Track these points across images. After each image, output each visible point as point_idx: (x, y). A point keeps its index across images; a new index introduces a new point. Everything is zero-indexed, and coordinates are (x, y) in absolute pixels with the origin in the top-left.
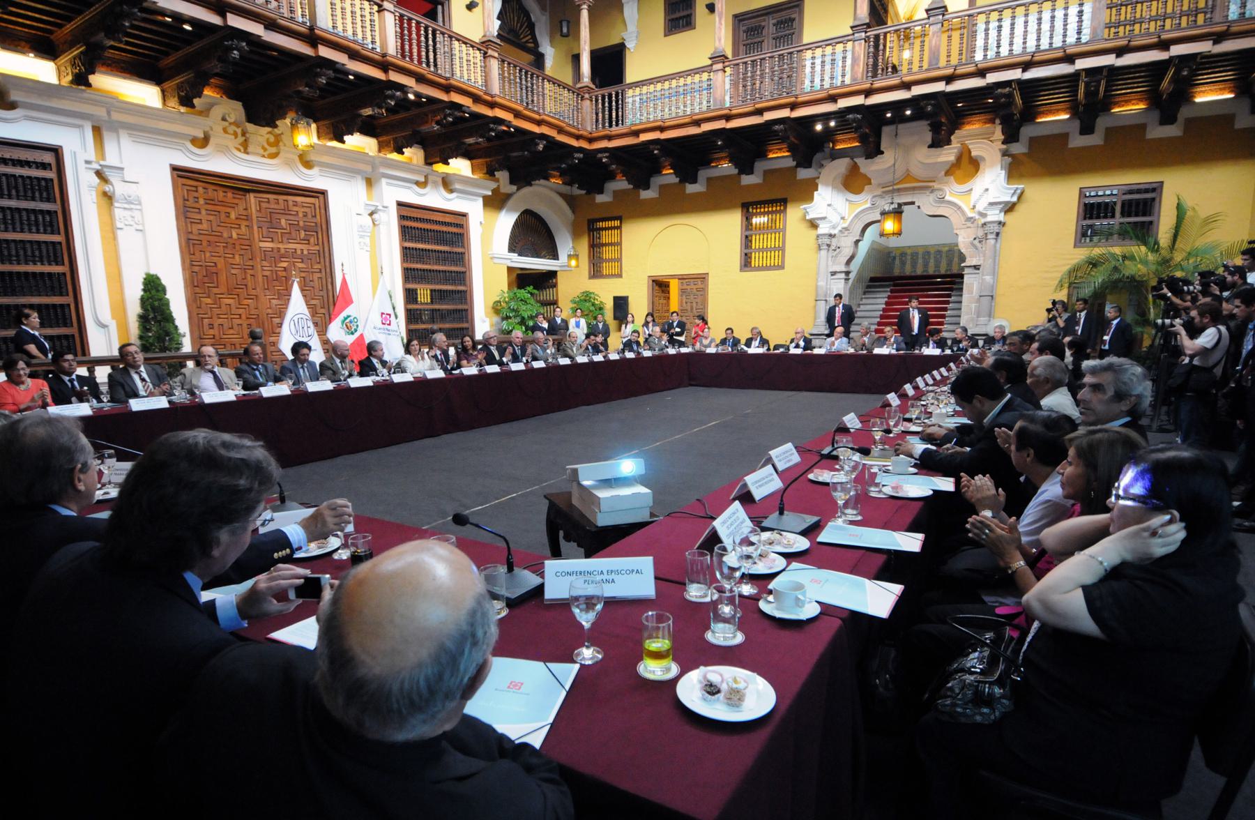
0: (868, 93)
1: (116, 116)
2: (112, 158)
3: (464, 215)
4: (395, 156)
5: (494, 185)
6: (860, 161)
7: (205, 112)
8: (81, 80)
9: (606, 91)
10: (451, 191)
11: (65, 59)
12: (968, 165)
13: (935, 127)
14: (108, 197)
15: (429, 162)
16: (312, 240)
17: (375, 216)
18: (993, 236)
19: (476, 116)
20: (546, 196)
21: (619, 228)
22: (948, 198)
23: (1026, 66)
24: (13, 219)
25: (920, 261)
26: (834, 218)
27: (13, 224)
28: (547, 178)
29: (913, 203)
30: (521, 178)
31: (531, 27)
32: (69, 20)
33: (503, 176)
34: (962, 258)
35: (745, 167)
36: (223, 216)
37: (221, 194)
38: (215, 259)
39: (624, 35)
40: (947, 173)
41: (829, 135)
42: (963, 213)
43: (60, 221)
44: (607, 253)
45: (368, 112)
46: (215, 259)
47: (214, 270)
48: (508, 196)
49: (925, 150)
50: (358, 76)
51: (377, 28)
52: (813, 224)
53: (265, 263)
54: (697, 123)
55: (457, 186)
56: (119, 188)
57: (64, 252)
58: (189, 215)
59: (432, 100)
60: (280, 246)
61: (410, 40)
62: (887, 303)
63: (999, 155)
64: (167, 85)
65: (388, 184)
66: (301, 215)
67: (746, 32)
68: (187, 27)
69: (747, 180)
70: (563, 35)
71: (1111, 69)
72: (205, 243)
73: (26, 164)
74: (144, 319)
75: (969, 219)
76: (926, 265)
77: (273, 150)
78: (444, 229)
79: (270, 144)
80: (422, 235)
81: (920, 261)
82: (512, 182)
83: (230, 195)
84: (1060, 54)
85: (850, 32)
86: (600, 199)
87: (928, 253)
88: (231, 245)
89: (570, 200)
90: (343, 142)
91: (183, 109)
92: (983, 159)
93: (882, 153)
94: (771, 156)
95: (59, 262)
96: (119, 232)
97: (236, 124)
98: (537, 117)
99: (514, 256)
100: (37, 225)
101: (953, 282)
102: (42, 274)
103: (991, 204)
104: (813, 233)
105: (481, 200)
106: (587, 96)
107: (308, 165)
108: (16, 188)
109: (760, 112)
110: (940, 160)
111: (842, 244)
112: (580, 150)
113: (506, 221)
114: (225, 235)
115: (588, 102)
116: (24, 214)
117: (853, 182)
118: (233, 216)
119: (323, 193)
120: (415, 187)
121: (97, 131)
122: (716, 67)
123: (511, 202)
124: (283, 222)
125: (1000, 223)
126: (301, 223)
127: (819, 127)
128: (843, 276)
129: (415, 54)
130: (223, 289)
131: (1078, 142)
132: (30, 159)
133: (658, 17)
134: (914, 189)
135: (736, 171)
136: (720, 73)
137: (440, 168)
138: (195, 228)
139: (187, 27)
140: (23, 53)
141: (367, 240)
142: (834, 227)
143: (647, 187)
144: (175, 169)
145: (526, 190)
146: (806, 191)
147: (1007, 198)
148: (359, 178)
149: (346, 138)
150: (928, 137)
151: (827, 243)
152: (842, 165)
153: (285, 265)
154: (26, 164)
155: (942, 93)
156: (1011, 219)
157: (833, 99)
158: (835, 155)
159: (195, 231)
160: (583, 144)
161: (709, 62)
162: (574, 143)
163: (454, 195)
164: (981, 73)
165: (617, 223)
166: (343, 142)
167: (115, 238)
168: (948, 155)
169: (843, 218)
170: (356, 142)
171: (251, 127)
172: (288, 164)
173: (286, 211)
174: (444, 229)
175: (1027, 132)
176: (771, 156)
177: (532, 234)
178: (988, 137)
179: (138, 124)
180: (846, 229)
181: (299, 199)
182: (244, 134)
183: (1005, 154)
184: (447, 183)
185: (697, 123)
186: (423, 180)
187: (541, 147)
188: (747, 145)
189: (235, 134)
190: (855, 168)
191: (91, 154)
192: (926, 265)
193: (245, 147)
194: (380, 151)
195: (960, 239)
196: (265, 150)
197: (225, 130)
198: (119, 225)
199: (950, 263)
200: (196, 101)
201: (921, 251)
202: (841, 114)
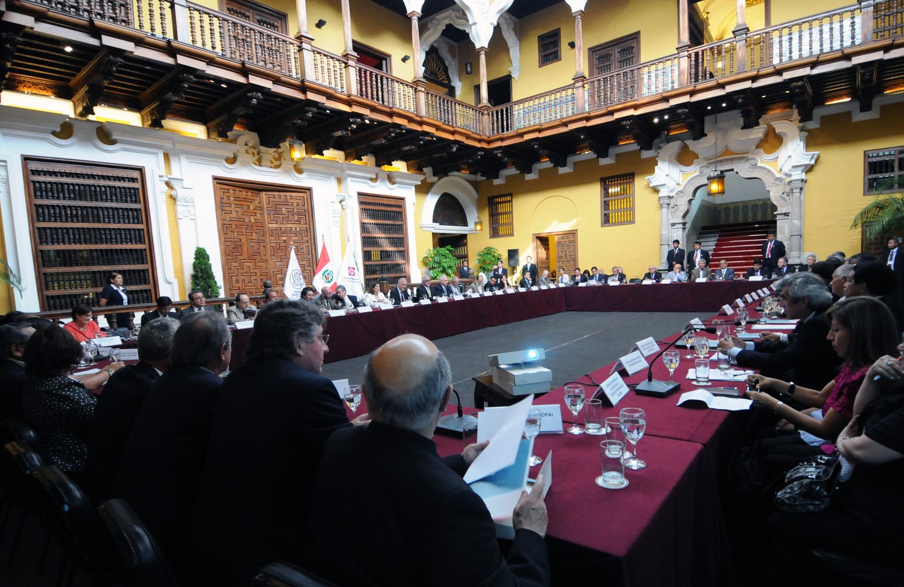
0: (692, 93)
3: (403, 199)
4: (356, 162)
5: (422, 177)
6: (690, 143)
7: (234, 141)
8: (156, 124)
9: (499, 108)
10: (393, 183)
11: (146, 111)
12: (773, 141)
13: (746, 115)
14: (173, 198)
15: (379, 164)
17: (343, 203)
18: (798, 190)
19: (410, 131)
20: (457, 183)
21: (511, 201)
22: (759, 164)
23: (813, 65)
24: (113, 215)
25: (741, 213)
26: (672, 185)
27: (114, 218)
28: (459, 171)
29: (732, 170)
30: (441, 171)
31: (446, 69)
32: (149, 85)
33: (428, 170)
34: (774, 208)
35: (602, 153)
36: (245, 208)
37: (244, 193)
38: (240, 237)
39: (510, 69)
40: (758, 147)
41: (664, 125)
42: (773, 174)
43: (142, 215)
44: (502, 219)
45: (339, 133)
46: (240, 237)
47: (239, 243)
48: (432, 184)
49: (739, 131)
50: (333, 111)
51: (344, 78)
52: (656, 190)
53: (272, 238)
54: (565, 124)
55: (398, 180)
56: (180, 193)
57: (145, 236)
58: (224, 208)
59: (381, 123)
61: (366, 85)
62: (716, 245)
63: (797, 131)
64: (211, 124)
67: (598, 59)
68: (224, 86)
69: (603, 162)
70: (468, 73)
71: (881, 62)
72: (234, 226)
74: (195, 277)
75: (778, 179)
76: (746, 215)
77: (277, 163)
78: (389, 209)
79: (275, 159)
81: (741, 213)
82: (435, 174)
83: (249, 194)
84: (839, 54)
85: (676, 52)
86: (496, 182)
87: (747, 206)
88: (249, 226)
90: (323, 155)
91: (220, 139)
92: (785, 134)
93: (706, 135)
94: (621, 143)
95: (141, 241)
97: (253, 147)
98: (451, 129)
99: (437, 225)
100: (129, 218)
101: (770, 226)
102: (131, 250)
103: (794, 167)
104: (656, 196)
105: (414, 188)
106: (486, 112)
107: (300, 171)
108: (116, 195)
109: (611, 113)
110: (752, 137)
111: (679, 203)
112: (482, 149)
113: (431, 201)
114: (247, 220)
115: (487, 117)
116: (121, 211)
117: (684, 158)
118: (251, 208)
119: (309, 189)
120: (370, 182)
122: (577, 85)
123: (434, 188)
124: (284, 210)
125: (802, 180)
127: (656, 120)
128: (681, 226)
129: (369, 93)
130: (245, 256)
131: (859, 117)
132: (125, 176)
133: (534, 54)
134: (732, 159)
135: (595, 156)
136: (581, 89)
137: (386, 168)
138: (228, 217)
139: (224, 86)
140: (121, 108)
141: (338, 219)
142: (672, 191)
143: (530, 172)
144: (219, 181)
145: (445, 179)
146: (649, 167)
147: (807, 162)
148: (333, 178)
149: (324, 152)
150: (741, 122)
151: (668, 203)
152: (675, 146)
153: (285, 238)
155: (750, 89)
156: (810, 177)
157: (666, 99)
158: (669, 140)
159: (228, 219)
160: (484, 145)
161: (573, 82)
162: (477, 145)
163: (396, 185)
164: (779, 72)
165: (509, 198)
166: (323, 155)
167: (177, 225)
168: (757, 133)
169: (678, 184)
170: (330, 154)
171: (263, 149)
172: (287, 171)
173: (286, 203)
174: (389, 209)
175: (818, 112)
176: (621, 143)
177: (449, 209)
178: (788, 118)
179: (191, 149)
180: (681, 192)
181: (294, 194)
182: (258, 154)
183: (802, 130)
184: (391, 178)
185: (565, 124)
187: (454, 149)
188: (602, 137)
189: (253, 154)
190: (685, 148)
191: (163, 171)
192: (746, 215)
193: (259, 162)
194: (346, 159)
195: (772, 194)
196: (272, 163)
197: (247, 152)
199: (765, 212)
200: (229, 134)
201: (741, 206)
202: (672, 110)
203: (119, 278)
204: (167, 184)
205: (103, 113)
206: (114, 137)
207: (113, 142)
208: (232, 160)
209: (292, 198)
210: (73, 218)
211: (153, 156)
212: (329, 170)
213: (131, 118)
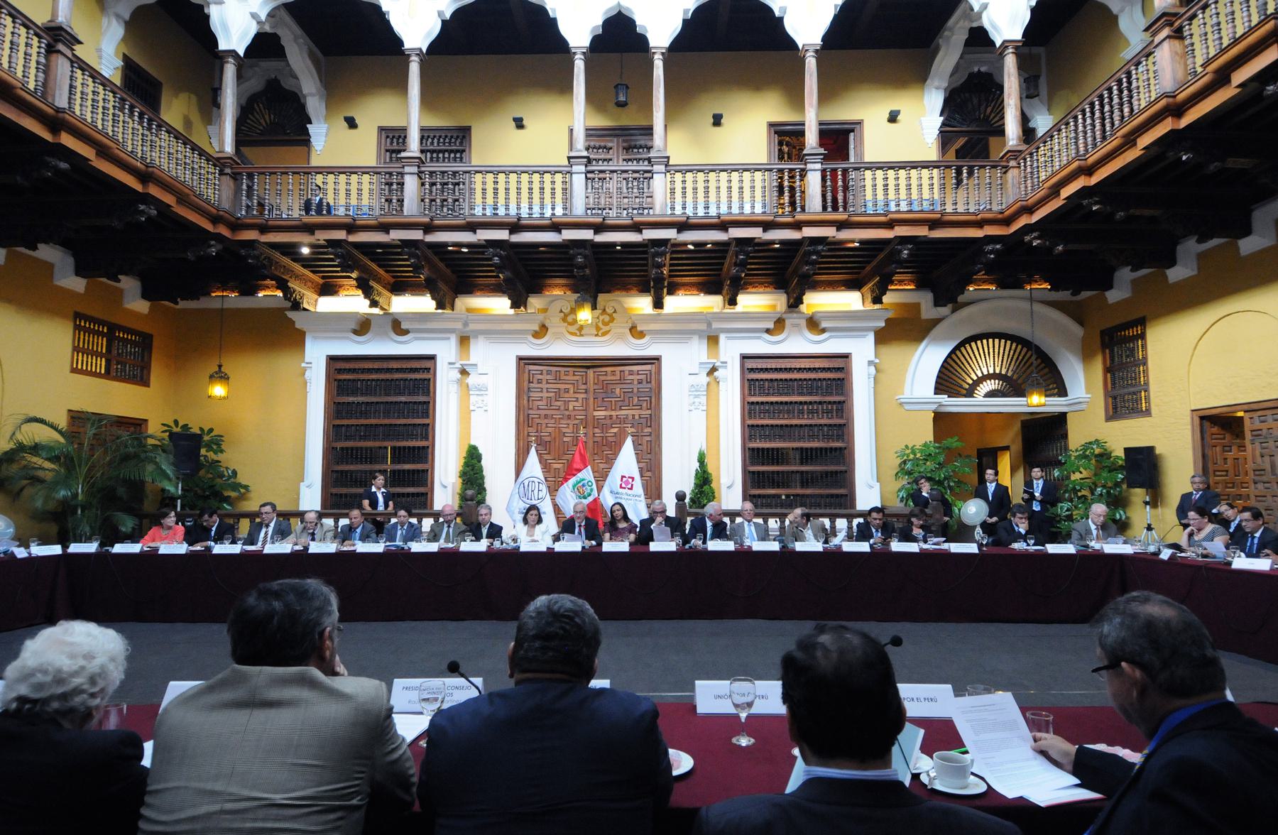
1: (472, 327)
3: (846, 356)
10: (824, 331)
30: (948, 295)
47: (548, 439)
48: (935, 322)
55: (824, 325)
60: (613, 413)
65: (729, 338)
73: (370, 371)
82: (938, 303)
89: (1076, 313)
99: (943, 398)
105: (871, 337)
107: (641, 335)
119: (656, 360)
120: (766, 336)
121: (464, 341)
124: (618, 391)
141: (704, 400)
148: (696, 338)
153: (615, 430)
172: (620, 337)
173: (622, 380)
181: (635, 368)
186: (771, 325)
203: (380, 480)
204: (464, 372)
205: (404, 304)
206: (404, 326)
207: (406, 332)
208: (541, 332)
209: (631, 373)
210: (365, 415)
212: (684, 328)
213: (423, 303)
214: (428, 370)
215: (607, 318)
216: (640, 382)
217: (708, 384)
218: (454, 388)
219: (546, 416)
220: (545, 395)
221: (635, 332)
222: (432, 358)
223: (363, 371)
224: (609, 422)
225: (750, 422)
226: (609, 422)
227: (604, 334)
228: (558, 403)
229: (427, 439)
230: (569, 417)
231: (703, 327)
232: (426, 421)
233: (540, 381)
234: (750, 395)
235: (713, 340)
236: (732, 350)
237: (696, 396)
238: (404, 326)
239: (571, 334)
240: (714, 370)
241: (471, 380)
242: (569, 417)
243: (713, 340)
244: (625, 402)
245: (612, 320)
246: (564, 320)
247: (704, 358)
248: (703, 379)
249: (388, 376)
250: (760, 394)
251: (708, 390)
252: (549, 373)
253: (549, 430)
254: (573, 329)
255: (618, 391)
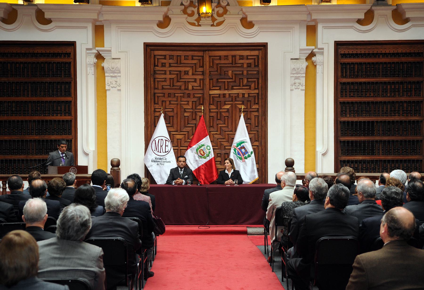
2: (107, 46)
10: (406, 21)
16: (253, 85)
53: (212, 107)
55: (408, 15)
56: (105, 64)
58: (157, 76)
60: (226, 92)
66: (245, 66)
73: (25, 55)
80: (371, 69)
96: (108, 92)
118: (190, 73)
119: (264, 47)
121: (99, 30)
124: (230, 73)
126: (245, 72)
141: (303, 81)
148: (297, 27)
153: (228, 107)
154: (25, 55)
186: (362, 17)
198: (107, 88)
204: (99, 57)
208: (164, 23)
209: (242, 58)
211: (84, 30)
214: (69, 55)
215: (221, 10)
216: (249, 65)
217: (307, 67)
218: (91, 70)
219: (169, 95)
220: (168, 76)
221: (247, 24)
222: (72, 44)
223: (13, 55)
224: (222, 99)
225: (341, 100)
226: (222, 99)
227: (219, 24)
228: (179, 84)
229: (70, 114)
230: (189, 96)
231: (304, 17)
232: (68, 99)
233: (163, 65)
234: (342, 76)
235: (312, 30)
236: (328, 38)
237: (297, 78)
238: (47, 16)
239: (193, 24)
240: (312, 54)
241: (105, 64)
242: (189, 96)
243: (312, 30)
244: (236, 81)
245: (225, 11)
246: (185, 12)
247: (303, 44)
248: (304, 64)
249: (34, 60)
250: (350, 77)
251: (306, 73)
252: (171, 57)
253: (173, 106)
254: (192, 19)
255: (230, 73)
